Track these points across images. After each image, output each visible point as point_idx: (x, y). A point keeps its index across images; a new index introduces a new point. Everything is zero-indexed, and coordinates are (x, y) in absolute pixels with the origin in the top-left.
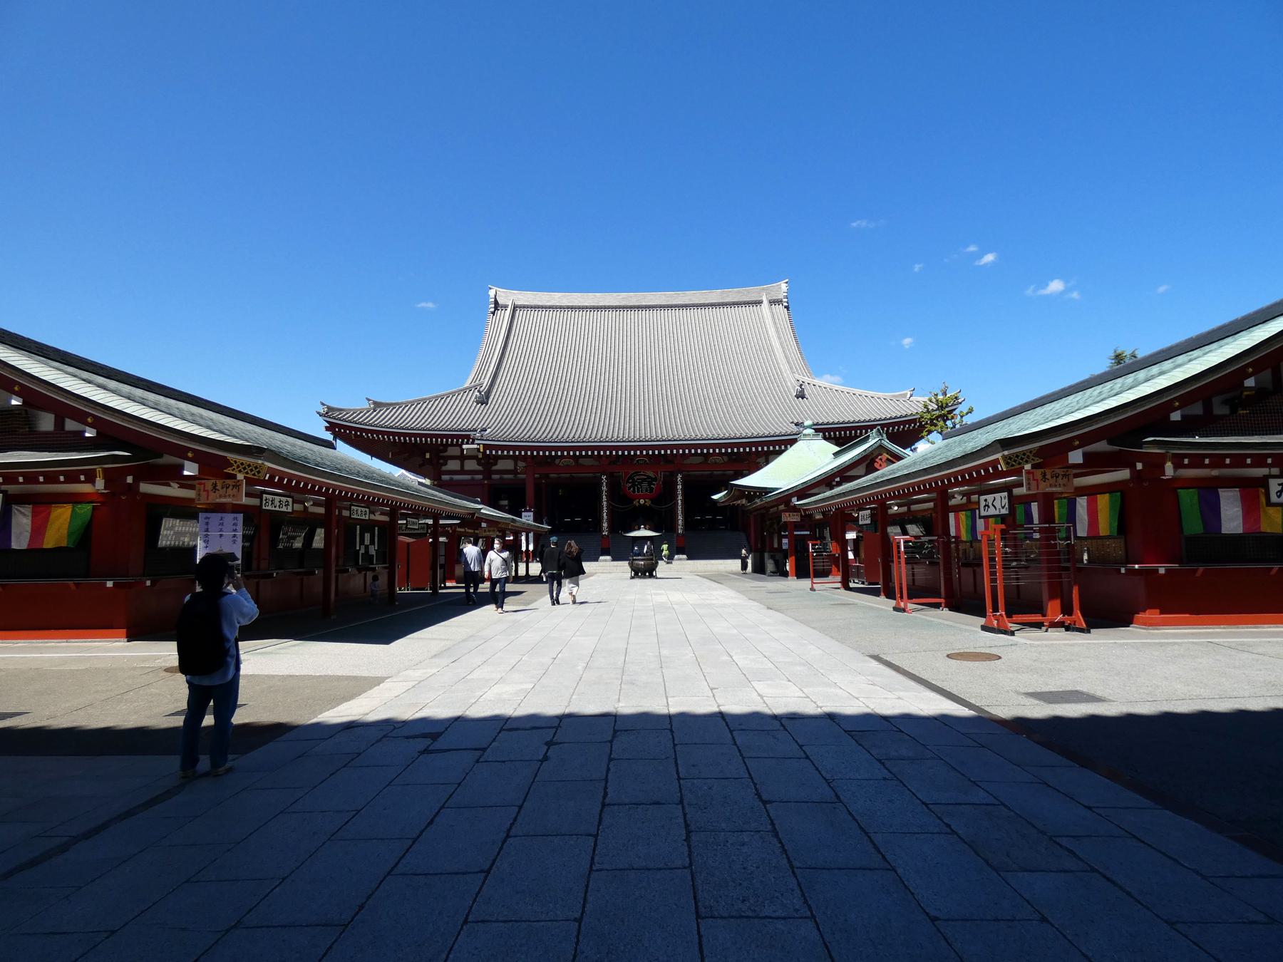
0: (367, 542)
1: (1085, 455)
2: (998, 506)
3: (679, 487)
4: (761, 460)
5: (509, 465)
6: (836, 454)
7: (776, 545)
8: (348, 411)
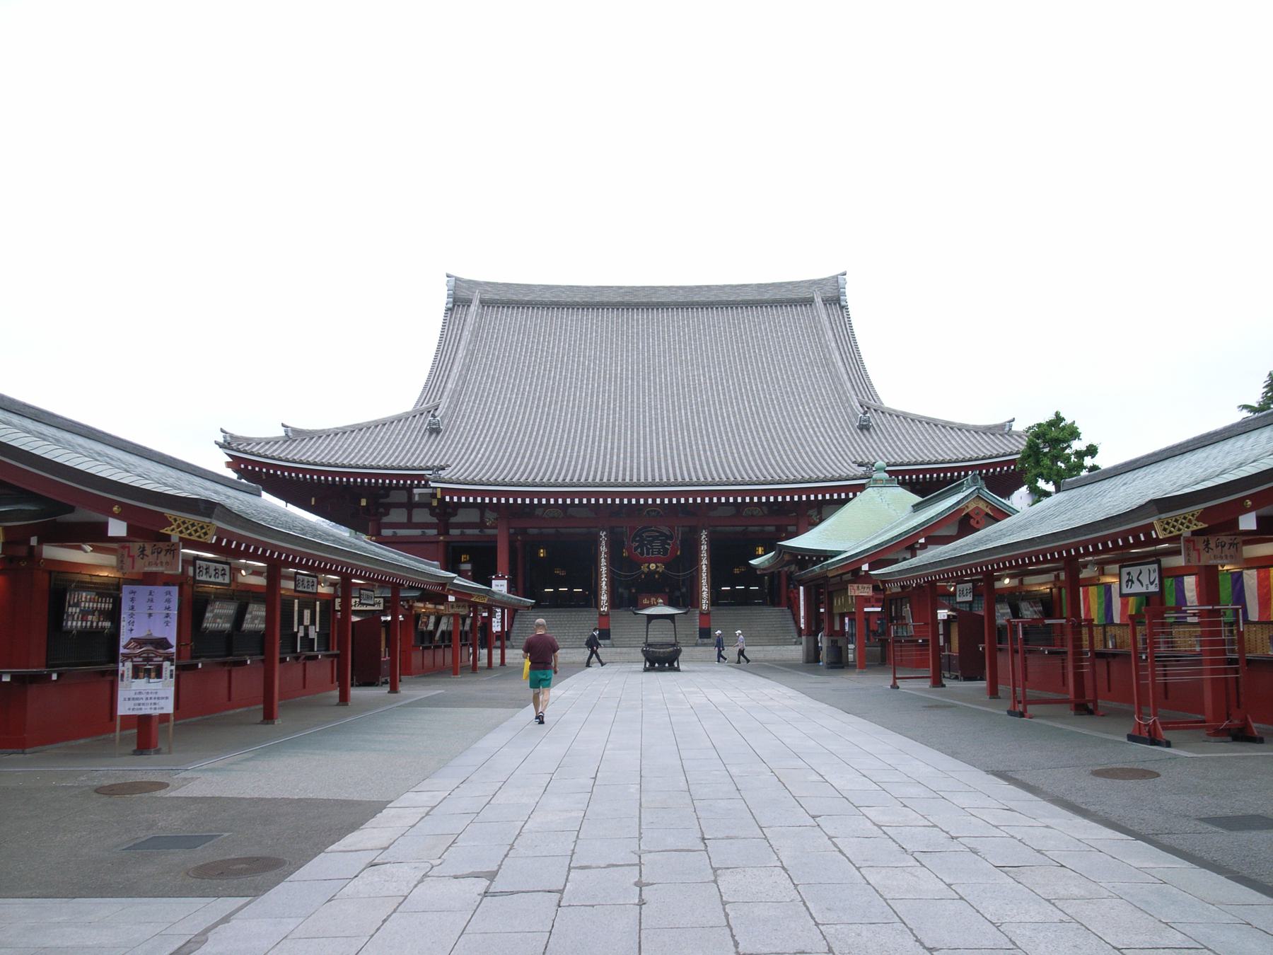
0: (307, 621)
1: (1259, 520)
2: (1146, 582)
3: (704, 547)
4: (813, 512)
5: (474, 516)
6: (917, 508)
7: (837, 628)
8: (259, 442)
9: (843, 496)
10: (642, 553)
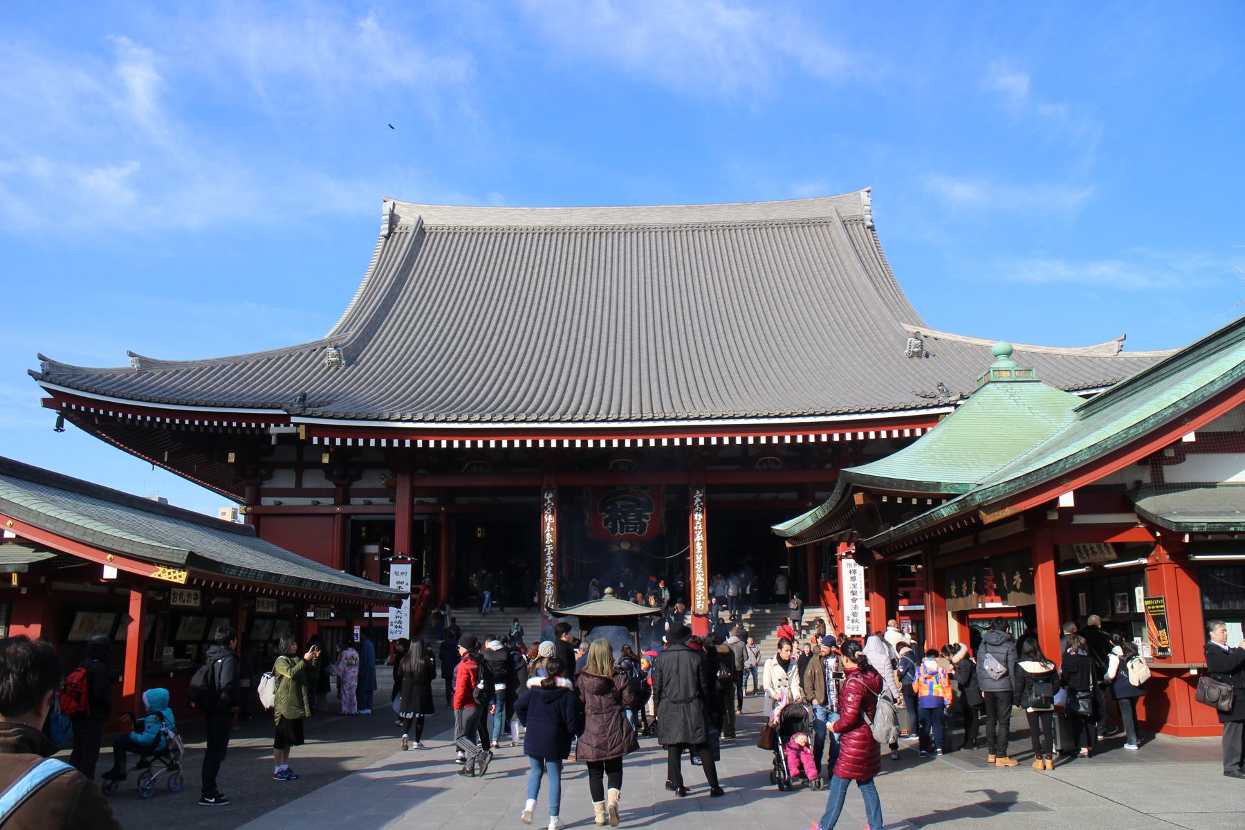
9: (907, 433)
10: (614, 529)
